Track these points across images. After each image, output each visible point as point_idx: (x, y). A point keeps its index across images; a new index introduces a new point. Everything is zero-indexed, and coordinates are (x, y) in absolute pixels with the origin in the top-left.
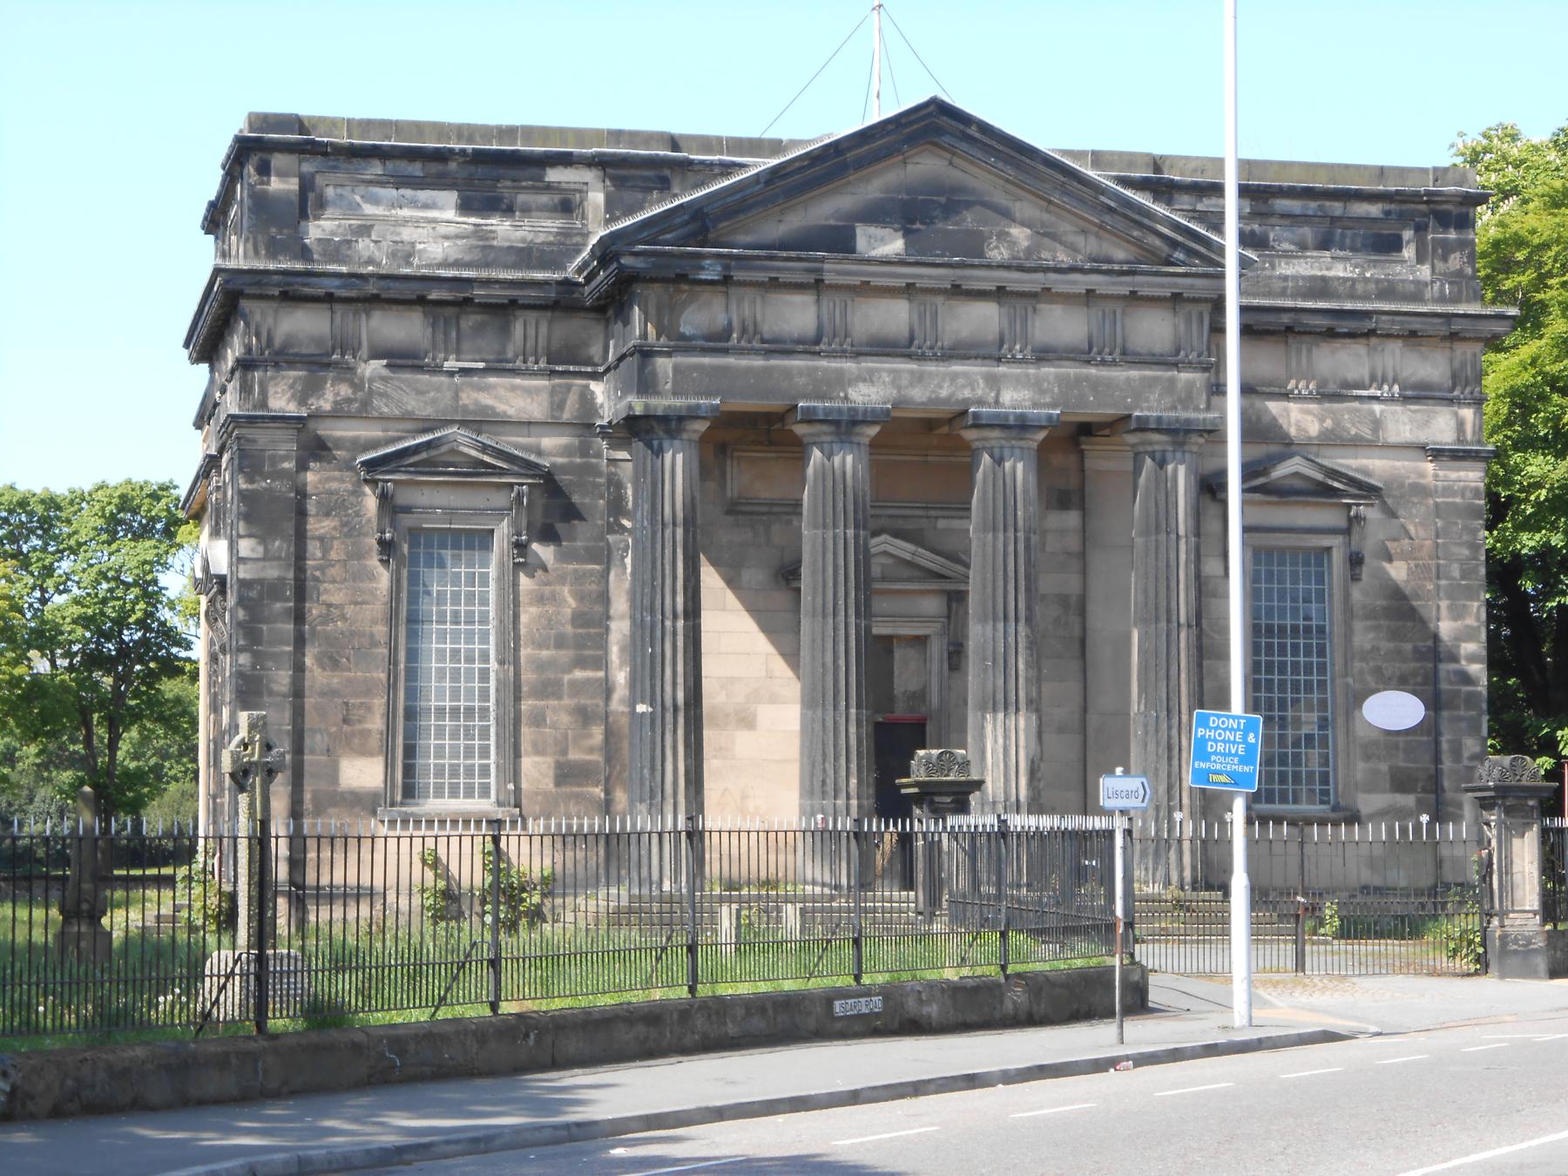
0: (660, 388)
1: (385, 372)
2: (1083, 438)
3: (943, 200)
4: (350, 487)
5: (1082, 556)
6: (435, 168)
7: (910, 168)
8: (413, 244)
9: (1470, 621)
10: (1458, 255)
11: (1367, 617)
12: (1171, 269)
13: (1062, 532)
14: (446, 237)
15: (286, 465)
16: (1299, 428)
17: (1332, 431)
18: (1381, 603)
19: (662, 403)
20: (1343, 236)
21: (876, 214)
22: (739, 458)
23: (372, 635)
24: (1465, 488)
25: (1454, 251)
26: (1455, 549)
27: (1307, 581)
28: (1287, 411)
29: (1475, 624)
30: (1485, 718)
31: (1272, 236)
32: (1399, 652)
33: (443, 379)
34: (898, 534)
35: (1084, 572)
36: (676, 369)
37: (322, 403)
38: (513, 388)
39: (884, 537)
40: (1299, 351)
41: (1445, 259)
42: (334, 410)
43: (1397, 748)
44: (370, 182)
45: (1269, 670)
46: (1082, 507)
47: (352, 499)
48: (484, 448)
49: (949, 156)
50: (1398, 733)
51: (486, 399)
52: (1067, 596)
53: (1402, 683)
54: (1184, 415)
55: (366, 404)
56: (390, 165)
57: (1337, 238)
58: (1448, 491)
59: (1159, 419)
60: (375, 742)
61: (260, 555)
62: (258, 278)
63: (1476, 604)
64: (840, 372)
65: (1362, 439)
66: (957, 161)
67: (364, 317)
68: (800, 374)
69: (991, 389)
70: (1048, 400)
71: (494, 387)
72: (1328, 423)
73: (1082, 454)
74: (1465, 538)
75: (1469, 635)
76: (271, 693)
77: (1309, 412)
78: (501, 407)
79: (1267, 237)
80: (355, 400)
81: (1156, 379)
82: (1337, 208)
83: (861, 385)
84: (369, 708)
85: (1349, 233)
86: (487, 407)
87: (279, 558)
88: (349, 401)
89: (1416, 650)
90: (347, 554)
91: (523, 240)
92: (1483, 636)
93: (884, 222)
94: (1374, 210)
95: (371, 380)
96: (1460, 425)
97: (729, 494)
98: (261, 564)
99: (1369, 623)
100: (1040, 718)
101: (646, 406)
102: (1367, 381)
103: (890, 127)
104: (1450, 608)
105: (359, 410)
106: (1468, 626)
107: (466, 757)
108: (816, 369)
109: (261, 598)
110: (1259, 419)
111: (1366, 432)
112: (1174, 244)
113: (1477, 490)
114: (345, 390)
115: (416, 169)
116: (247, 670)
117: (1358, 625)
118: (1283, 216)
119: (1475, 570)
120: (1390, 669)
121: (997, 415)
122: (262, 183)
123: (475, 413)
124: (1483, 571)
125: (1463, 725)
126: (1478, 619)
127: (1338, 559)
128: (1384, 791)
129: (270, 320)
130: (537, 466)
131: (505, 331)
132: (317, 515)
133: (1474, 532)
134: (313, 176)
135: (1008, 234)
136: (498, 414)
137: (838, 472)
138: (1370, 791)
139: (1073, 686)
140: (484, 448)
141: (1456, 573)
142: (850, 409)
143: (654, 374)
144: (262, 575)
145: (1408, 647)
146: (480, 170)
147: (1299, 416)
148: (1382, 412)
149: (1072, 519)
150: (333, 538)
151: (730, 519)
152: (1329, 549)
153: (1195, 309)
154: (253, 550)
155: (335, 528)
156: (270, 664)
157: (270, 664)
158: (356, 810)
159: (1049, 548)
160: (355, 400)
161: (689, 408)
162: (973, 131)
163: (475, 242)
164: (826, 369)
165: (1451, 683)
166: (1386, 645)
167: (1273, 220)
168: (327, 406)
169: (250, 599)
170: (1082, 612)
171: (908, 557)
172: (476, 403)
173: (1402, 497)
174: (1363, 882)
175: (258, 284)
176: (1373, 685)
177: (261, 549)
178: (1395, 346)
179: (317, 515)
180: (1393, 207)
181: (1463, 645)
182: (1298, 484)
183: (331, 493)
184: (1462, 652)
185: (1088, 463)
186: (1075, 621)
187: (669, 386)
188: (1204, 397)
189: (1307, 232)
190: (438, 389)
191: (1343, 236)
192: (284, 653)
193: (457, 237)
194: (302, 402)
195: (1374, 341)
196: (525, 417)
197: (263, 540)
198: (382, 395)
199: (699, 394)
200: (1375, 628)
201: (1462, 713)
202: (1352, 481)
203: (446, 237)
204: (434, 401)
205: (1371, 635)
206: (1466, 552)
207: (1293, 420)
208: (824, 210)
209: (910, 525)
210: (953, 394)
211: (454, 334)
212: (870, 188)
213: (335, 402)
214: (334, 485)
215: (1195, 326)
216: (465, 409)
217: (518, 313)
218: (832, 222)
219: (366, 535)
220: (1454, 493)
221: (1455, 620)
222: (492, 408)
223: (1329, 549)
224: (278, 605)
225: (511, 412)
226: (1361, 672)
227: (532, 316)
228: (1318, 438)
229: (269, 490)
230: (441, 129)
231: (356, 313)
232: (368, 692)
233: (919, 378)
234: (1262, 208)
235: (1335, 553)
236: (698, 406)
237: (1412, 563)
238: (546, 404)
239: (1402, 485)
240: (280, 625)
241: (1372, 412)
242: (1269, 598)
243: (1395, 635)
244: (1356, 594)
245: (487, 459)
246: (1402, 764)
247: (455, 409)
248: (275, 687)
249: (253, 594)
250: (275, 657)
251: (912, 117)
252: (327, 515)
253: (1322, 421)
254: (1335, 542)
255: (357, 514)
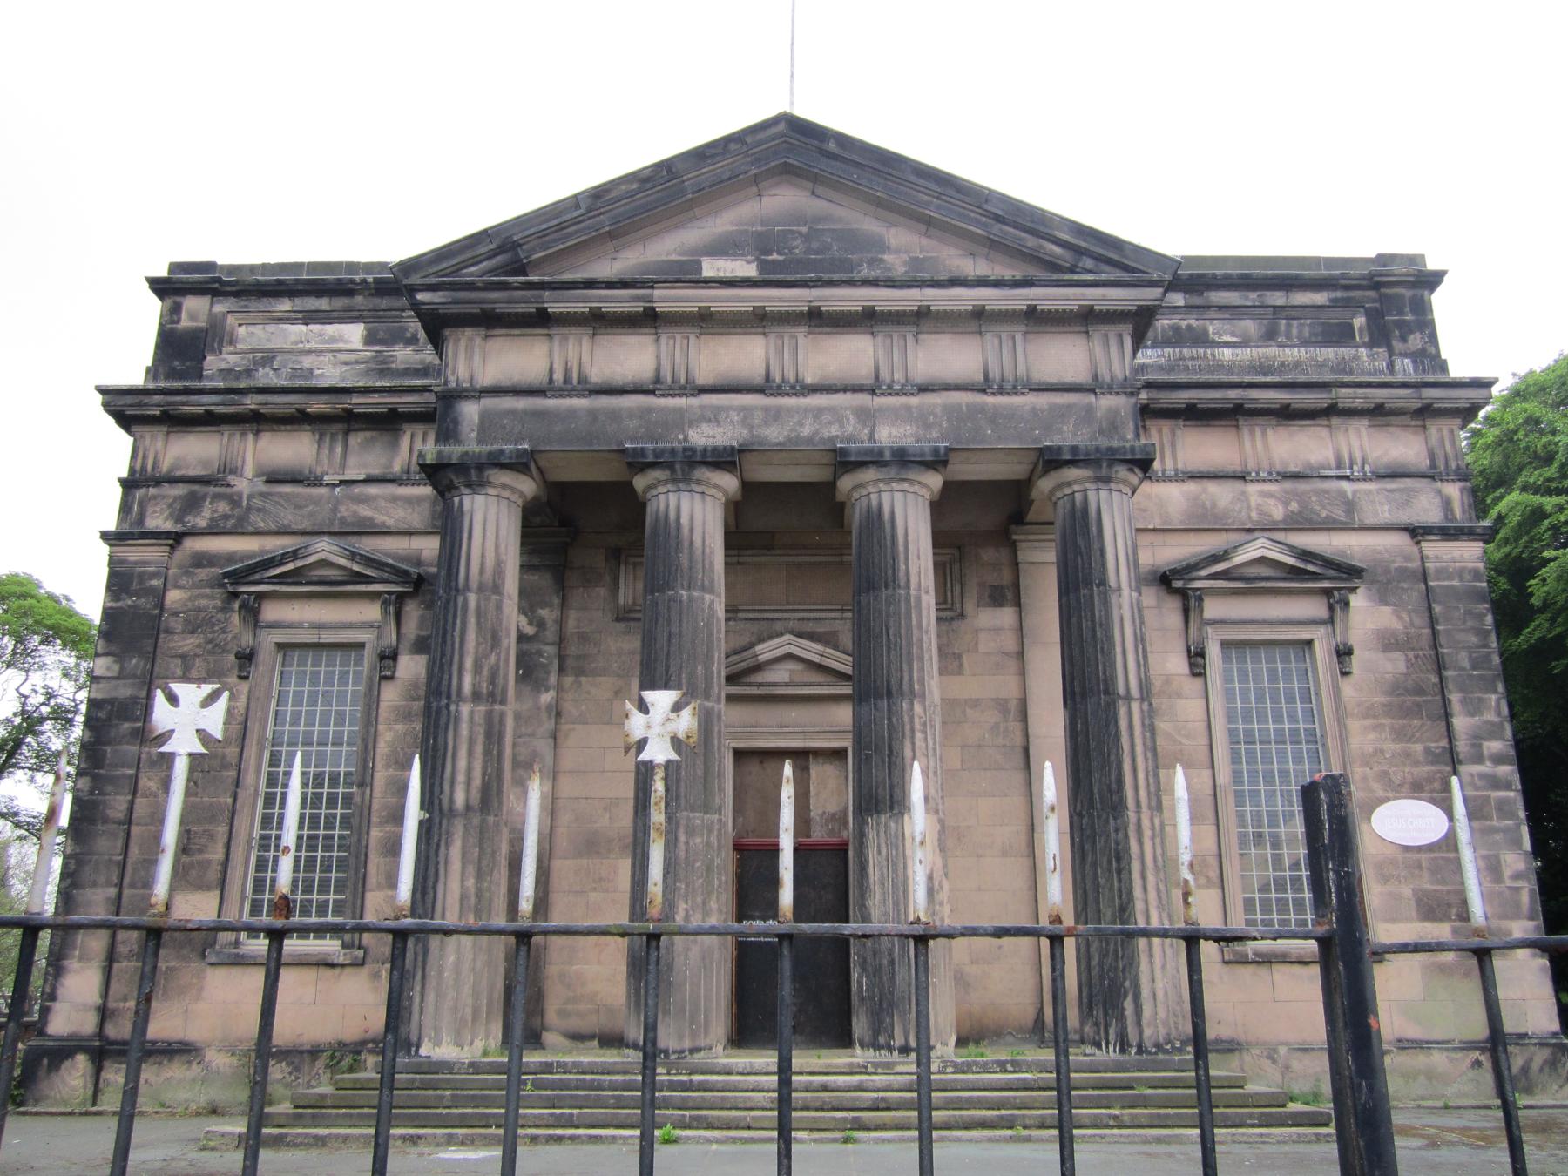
0: (463, 437)
1: (265, 488)
2: (1013, 527)
3: (804, 230)
4: (219, 603)
5: (1021, 655)
6: (340, 302)
7: (765, 199)
8: (311, 371)
9: (1491, 716)
10: (1418, 335)
11: (1366, 716)
12: (1076, 277)
13: (997, 630)
14: (346, 363)
15: (154, 582)
16: (1261, 512)
17: (1300, 513)
18: (1383, 699)
19: (454, 451)
20: (1289, 326)
21: (722, 248)
22: (635, 565)
23: (224, 757)
24: (1463, 570)
25: (1412, 332)
26: (1461, 637)
27: (1288, 679)
28: (1243, 493)
29: (1497, 720)
30: (1525, 830)
31: (1211, 330)
32: (1407, 755)
33: (323, 491)
34: (800, 635)
35: (1023, 673)
36: (485, 416)
37: (198, 520)
38: (395, 499)
39: (787, 637)
40: (1252, 433)
41: (1404, 339)
42: (209, 527)
43: (1420, 867)
44: (280, 319)
45: (1253, 780)
46: (1018, 603)
47: (220, 616)
48: (353, 556)
49: (810, 185)
50: (1419, 849)
51: (364, 511)
52: (1006, 700)
53: (1416, 789)
54: (1104, 443)
55: (242, 520)
56: (298, 301)
57: (1283, 328)
58: (1442, 573)
59: (1074, 449)
60: (213, 874)
61: (115, 674)
62: (140, 398)
63: (1494, 697)
64: (680, 411)
65: (1335, 521)
66: (820, 190)
67: (250, 437)
68: (631, 415)
69: (865, 425)
70: (935, 435)
71: (374, 498)
72: (1294, 506)
73: (1013, 547)
74: (1470, 623)
75: (1493, 732)
76: (106, 820)
77: (1270, 495)
78: (380, 518)
79: (1206, 332)
80: (232, 516)
81: (1069, 406)
82: (1278, 298)
83: (704, 427)
84: (211, 836)
85: (1295, 323)
86: (365, 518)
87: (134, 676)
88: (226, 517)
89: (1427, 751)
90: (208, 672)
91: (422, 362)
92: (1508, 733)
93: (735, 254)
94: (1320, 298)
95: (250, 497)
96: (1447, 504)
97: (621, 601)
98: (114, 682)
99: (1368, 722)
100: (941, 821)
101: (440, 453)
102: (1333, 464)
103: (732, 146)
104: (1463, 702)
105: (235, 526)
106: (1487, 722)
107: (319, 893)
108: (649, 410)
109: (109, 719)
110: (1214, 505)
111: (1339, 514)
112: (1079, 252)
113: (1476, 575)
114: (223, 507)
115: (323, 304)
116: (85, 796)
117: (1354, 726)
118: (1221, 308)
119: (1487, 657)
120: (1400, 773)
121: (870, 451)
122: (173, 322)
123: (352, 524)
124: (1496, 660)
125: (1498, 837)
126: (1499, 714)
127: (1323, 651)
128: (1408, 920)
129: (160, 444)
130: (406, 573)
131: (394, 445)
132: (183, 632)
133: (1481, 616)
134: (224, 315)
135: (881, 260)
136: (376, 525)
137: (673, 525)
138: (1393, 920)
139: (1017, 801)
140: (353, 556)
141: (1466, 664)
142: (685, 449)
143: (456, 422)
144: (113, 694)
145: (1419, 747)
146: (384, 303)
147: (1260, 500)
148: (1354, 493)
149: (1006, 616)
150: (196, 655)
151: (621, 626)
152: (1309, 643)
153: (1112, 331)
154: (108, 669)
155: (199, 646)
156: (109, 788)
157: (109, 788)
158: (185, 952)
159: (982, 648)
160: (232, 516)
161: (490, 453)
162: (832, 146)
163: (373, 366)
164: (663, 410)
165: (1477, 788)
166: (1391, 747)
167: (1212, 313)
168: (202, 522)
169: (98, 719)
170: (1024, 717)
171: (816, 659)
172: (355, 513)
173: (1389, 582)
174: (1397, 1035)
175: (139, 405)
176: (1381, 793)
177: (116, 667)
178: (1360, 426)
179: (183, 632)
180: (1339, 294)
181: (1486, 744)
182: (1265, 571)
183: (199, 610)
184: (1486, 752)
185: (1021, 557)
186: (1016, 727)
187: (474, 435)
188: (1131, 426)
189: (1250, 326)
190: (317, 501)
191: (1289, 326)
192: (124, 776)
193: (357, 362)
194: (179, 520)
195: (1335, 421)
196: (403, 527)
197: (119, 657)
198: (259, 510)
199: (508, 442)
200: (1375, 728)
201: (1495, 823)
202: (1328, 563)
203: (346, 363)
204: (311, 515)
205: (1372, 736)
206: (1474, 639)
207: (1253, 504)
208: (664, 247)
209: (820, 628)
210: (817, 432)
211: (339, 450)
212: (719, 221)
213: (212, 519)
214: (203, 602)
215: (1114, 350)
216: (343, 521)
217: (405, 426)
218: (674, 257)
219: (228, 652)
220: (1450, 577)
221: (1472, 715)
222: (371, 519)
223: (1309, 643)
224: (126, 725)
225: (390, 522)
226: (1365, 779)
227: (419, 429)
228: (1284, 521)
229: (135, 607)
230: (352, 267)
231: (243, 434)
232: (212, 819)
233: (775, 415)
234: (1197, 300)
235: (1317, 644)
236: (502, 452)
237: (1411, 654)
238: (427, 513)
239: (1387, 571)
240: (125, 747)
241: (1342, 494)
242: (1245, 699)
243: (1399, 735)
244: (1348, 688)
245: (356, 567)
246: (1428, 886)
247: (332, 523)
248: (111, 814)
249: (102, 715)
250: (113, 780)
251: (761, 136)
252: (192, 632)
253: (1286, 504)
254: (1319, 635)
255: (224, 631)
